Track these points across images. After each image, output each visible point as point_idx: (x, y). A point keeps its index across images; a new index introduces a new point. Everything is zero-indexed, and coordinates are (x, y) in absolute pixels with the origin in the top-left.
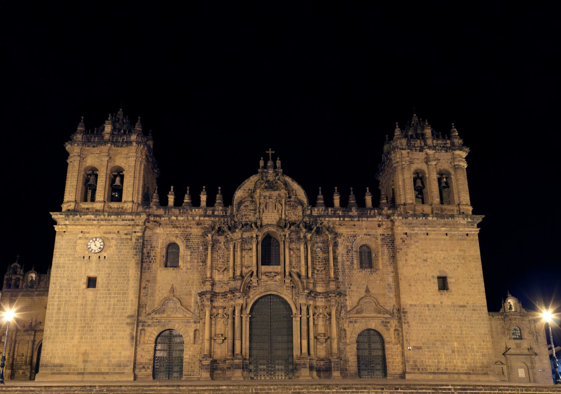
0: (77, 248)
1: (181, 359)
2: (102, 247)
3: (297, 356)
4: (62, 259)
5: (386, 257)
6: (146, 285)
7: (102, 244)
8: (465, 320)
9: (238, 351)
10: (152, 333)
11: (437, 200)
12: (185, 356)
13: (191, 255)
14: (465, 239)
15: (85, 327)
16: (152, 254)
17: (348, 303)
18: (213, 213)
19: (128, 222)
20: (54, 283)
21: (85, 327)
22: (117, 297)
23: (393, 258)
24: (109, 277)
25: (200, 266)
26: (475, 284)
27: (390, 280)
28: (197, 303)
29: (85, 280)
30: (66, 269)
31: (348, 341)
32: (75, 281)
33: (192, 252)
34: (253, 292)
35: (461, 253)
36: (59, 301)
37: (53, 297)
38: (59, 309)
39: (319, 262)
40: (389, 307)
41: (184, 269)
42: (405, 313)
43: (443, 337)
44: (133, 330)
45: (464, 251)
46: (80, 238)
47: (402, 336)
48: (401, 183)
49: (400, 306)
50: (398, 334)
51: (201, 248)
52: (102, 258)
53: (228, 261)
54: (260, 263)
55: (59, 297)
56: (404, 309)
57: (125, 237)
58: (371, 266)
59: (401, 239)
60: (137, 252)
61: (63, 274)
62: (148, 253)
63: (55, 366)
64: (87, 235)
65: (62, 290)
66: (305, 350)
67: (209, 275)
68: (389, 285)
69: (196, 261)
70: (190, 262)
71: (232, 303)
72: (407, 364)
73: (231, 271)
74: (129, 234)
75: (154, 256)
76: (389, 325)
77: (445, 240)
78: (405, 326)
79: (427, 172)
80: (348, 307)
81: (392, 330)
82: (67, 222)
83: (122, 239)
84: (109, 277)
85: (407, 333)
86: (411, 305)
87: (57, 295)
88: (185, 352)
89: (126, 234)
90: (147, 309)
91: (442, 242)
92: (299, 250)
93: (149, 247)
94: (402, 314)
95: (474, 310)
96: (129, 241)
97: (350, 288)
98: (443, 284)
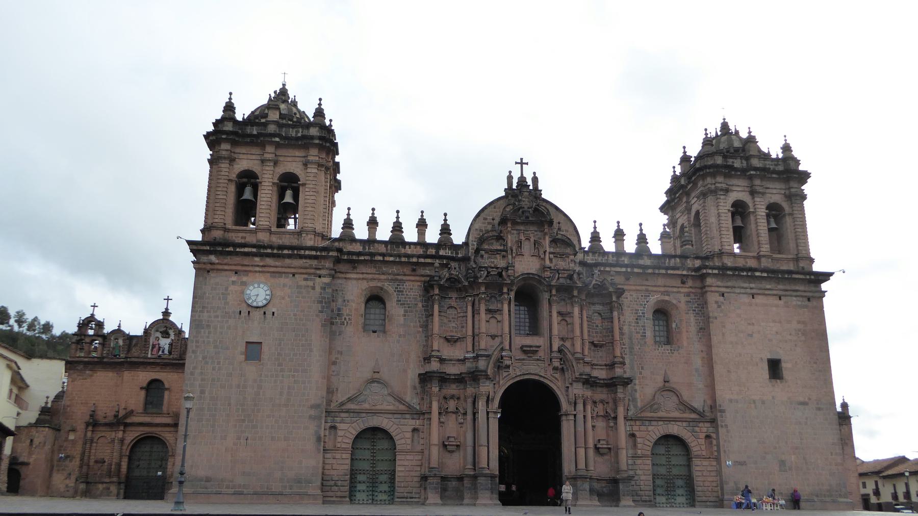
0: (230, 298)
1: (393, 474)
2: (268, 297)
3: (570, 472)
4: (205, 314)
5: (693, 329)
6: (337, 358)
7: (268, 292)
8: (806, 423)
9: (484, 464)
10: (348, 430)
11: (766, 248)
12: (398, 469)
13: (405, 315)
14: (806, 307)
15: (243, 421)
16: (345, 311)
17: (638, 395)
18: (437, 252)
19: (308, 261)
20: (193, 352)
21: (243, 421)
22: (293, 376)
23: (704, 330)
24: (280, 344)
25: (419, 332)
26: (820, 371)
27: (698, 362)
28: (415, 388)
29: (242, 347)
30: (212, 330)
31: (639, 452)
32: (227, 349)
33: (406, 311)
34: (505, 374)
35: (801, 326)
36: (203, 380)
37: (192, 374)
38: (202, 392)
39: (596, 333)
40: (697, 404)
42: (723, 411)
43: (775, 448)
44: (319, 427)
45: (804, 323)
46: (234, 283)
47: (718, 445)
48: (713, 219)
49: (715, 401)
50: (711, 443)
51: (420, 305)
52: (269, 315)
55: (202, 373)
56: (720, 406)
57: (304, 283)
58: (669, 341)
59: (717, 302)
60: (323, 307)
61: (208, 337)
62: (339, 310)
63: (201, 480)
64: (245, 279)
65: (207, 363)
66: (582, 465)
68: (697, 370)
71: (470, 390)
72: (725, 486)
73: (470, 340)
74: (311, 280)
75: (348, 315)
76: (697, 429)
77: (777, 306)
78: (722, 431)
79: (751, 205)
80: (639, 400)
81: (703, 435)
82: (213, 258)
83: (299, 287)
84: (280, 344)
85: (725, 441)
86: (731, 401)
87: (198, 371)
88: (398, 463)
89: (306, 279)
90: (339, 395)
91: (774, 309)
92: (570, 314)
93: (340, 300)
94: (719, 414)
95: (819, 409)
96: (310, 289)
97: (641, 373)
98: (775, 368)
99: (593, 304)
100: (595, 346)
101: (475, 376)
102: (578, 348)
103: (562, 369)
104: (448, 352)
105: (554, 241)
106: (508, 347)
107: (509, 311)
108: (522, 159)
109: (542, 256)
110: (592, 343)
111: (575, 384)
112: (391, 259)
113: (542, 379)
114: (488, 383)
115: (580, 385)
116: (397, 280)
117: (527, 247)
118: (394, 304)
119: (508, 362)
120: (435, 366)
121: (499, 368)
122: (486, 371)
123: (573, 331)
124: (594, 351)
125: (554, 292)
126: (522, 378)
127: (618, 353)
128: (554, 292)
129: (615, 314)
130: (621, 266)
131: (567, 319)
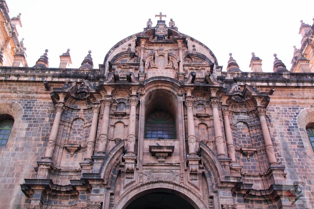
13: (28, 129)
33: (30, 125)
34: (127, 181)
39: (244, 142)
41: (11, 149)
51: (47, 119)
53: (87, 137)
54: (141, 135)
67: (48, 153)
69: (34, 138)
70: (25, 138)
99: (237, 113)
100: (245, 154)
101: (86, 183)
102: (222, 149)
103: (203, 174)
104: (66, 162)
105: (189, 56)
106: (132, 149)
107: (138, 115)
108: (161, 13)
109: (176, 67)
110: (241, 151)
111: (221, 192)
112: (26, 79)
113: (177, 189)
114: (103, 191)
115: (228, 193)
116: (29, 97)
117: (161, 62)
118: (20, 119)
119: (130, 165)
120: (43, 174)
121: (120, 173)
122: (99, 174)
123: (214, 134)
124: (243, 160)
125: (189, 94)
126: (151, 187)
127: (273, 158)
128: (189, 94)
129: (263, 118)
130: (262, 81)
131: (208, 123)
